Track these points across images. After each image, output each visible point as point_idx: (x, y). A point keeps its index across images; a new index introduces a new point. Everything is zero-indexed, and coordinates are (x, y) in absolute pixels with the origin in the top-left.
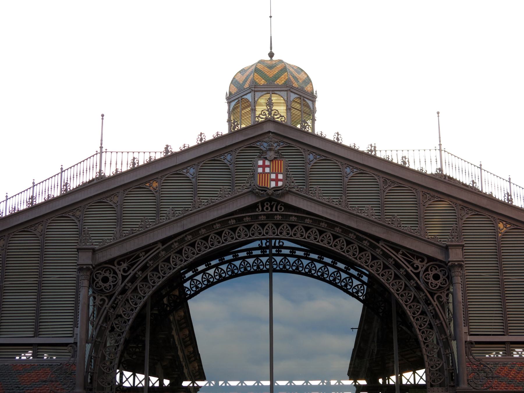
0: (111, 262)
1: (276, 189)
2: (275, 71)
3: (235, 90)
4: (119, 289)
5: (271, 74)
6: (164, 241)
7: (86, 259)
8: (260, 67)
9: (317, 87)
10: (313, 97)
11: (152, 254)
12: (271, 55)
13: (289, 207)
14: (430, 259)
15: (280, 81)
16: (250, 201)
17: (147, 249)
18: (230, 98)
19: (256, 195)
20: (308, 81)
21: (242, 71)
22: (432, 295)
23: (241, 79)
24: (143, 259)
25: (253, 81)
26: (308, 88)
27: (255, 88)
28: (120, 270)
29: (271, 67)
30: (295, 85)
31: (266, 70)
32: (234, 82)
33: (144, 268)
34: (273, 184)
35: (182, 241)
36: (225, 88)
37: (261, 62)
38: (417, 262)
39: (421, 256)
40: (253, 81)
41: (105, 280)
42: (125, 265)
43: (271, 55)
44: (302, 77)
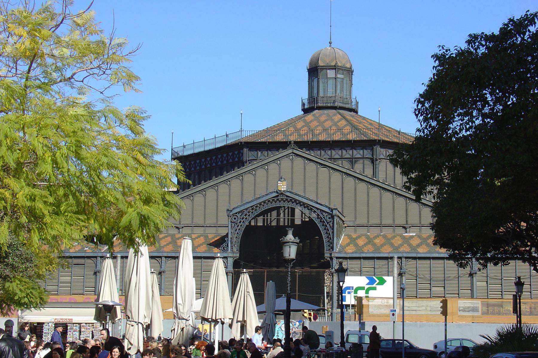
0: (236, 213)
1: (284, 191)
4: (239, 221)
6: (251, 207)
11: (248, 211)
13: (287, 196)
14: (328, 213)
16: (275, 194)
17: (246, 209)
19: (277, 193)
22: (328, 223)
24: (246, 212)
28: (238, 215)
33: (246, 215)
34: (283, 189)
35: (257, 207)
38: (324, 214)
39: (326, 212)
41: (235, 219)
42: (240, 214)
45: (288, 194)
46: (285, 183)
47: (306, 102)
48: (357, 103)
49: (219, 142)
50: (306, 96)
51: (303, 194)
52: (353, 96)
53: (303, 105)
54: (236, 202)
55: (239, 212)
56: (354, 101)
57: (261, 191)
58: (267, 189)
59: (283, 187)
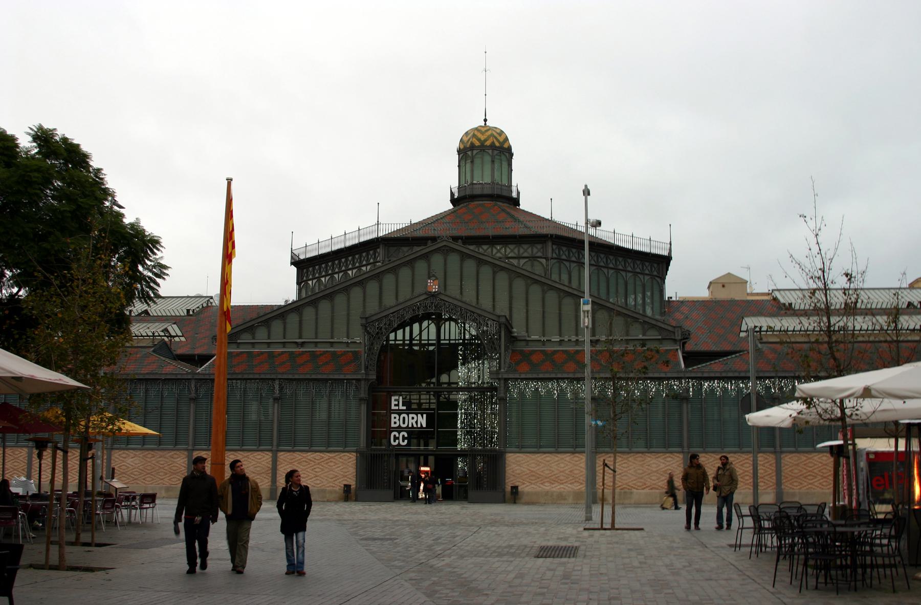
3: (462, 147)
5: (482, 138)
7: (364, 321)
8: (476, 133)
10: (510, 148)
12: (485, 120)
15: (488, 143)
16: (424, 297)
18: (460, 151)
20: (506, 139)
21: (467, 133)
23: (465, 139)
25: (472, 144)
26: (506, 146)
27: (473, 147)
30: (497, 144)
31: (479, 135)
36: (456, 145)
37: (476, 129)
40: (472, 144)
43: (485, 120)
44: (501, 139)
45: (443, 297)
46: (437, 282)
48: (518, 193)
49: (350, 239)
50: (455, 184)
51: (458, 297)
52: (514, 184)
53: (452, 194)
54: (373, 307)
55: (377, 320)
56: (514, 189)
57: (405, 293)
58: (413, 291)
59: (434, 286)
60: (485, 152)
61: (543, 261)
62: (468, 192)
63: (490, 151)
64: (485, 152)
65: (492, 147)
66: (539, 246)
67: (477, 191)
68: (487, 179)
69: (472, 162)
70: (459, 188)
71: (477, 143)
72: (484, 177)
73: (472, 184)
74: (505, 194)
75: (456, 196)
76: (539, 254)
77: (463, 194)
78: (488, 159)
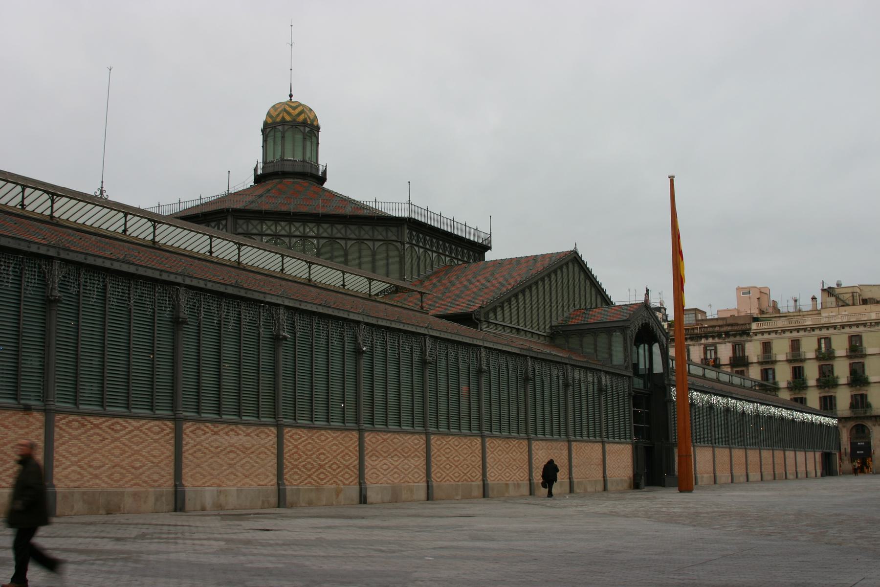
2: (297, 111)
3: (270, 121)
9: (321, 122)
10: (318, 129)
12: (291, 96)
21: (274, 107)
26: (315, 123)
27: (283, 122)
29: (294, 108)
32: (269, 114)
40: (283, 118)
43: (291, 96)
47: (261, 166)
53: (256, 170)
60: (292, 128)
61: (398, 245)
62: (278, 169)
63: (302, 128)
64: (292, 128)
65: (304, 123)
66: (394, 229)
67: (288, 168)
68: (299, 157)
69: (283, 137)
70: (265, 162)
71: (288, 118)
72: (293, 154)
73: (283, 160)
74: (314, 172)
75: (260, 172)
76: (394, 238)
77: (270, 170)
78: (299, 137)
